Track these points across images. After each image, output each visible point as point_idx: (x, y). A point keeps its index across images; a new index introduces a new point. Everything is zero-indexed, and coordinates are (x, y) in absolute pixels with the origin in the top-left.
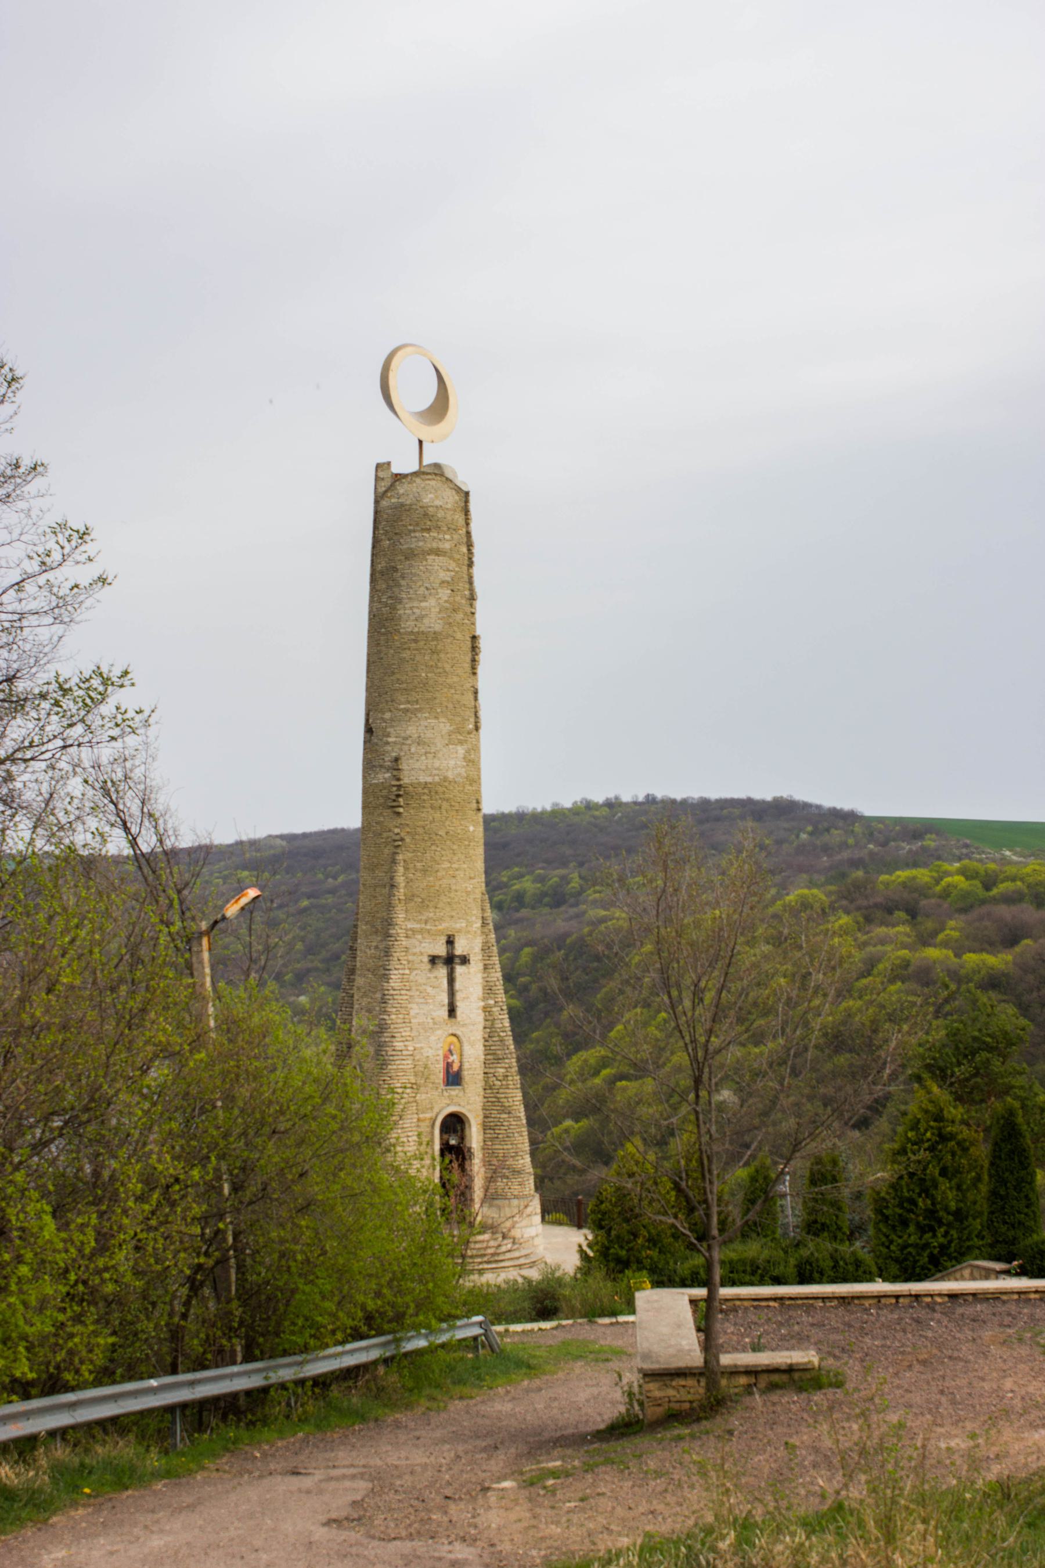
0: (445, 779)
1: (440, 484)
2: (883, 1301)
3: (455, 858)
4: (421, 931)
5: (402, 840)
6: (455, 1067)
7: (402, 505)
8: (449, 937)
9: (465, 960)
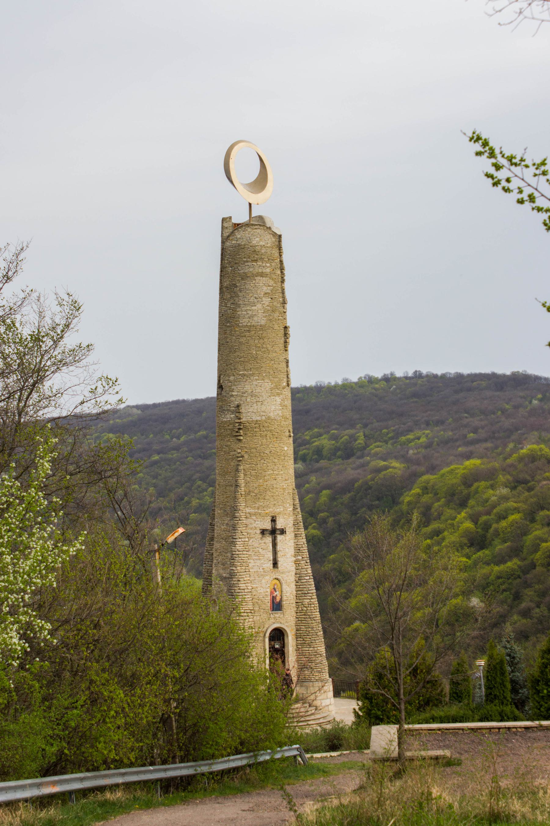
0: (269, 418)
1: (263, 231)
2: (492, 730)
3: (276, 468)
4: (255, 514)
5: (242, 457)
6: (278, 599)
7: (239, 245)
8: (273, 517)
9: (283, 532)
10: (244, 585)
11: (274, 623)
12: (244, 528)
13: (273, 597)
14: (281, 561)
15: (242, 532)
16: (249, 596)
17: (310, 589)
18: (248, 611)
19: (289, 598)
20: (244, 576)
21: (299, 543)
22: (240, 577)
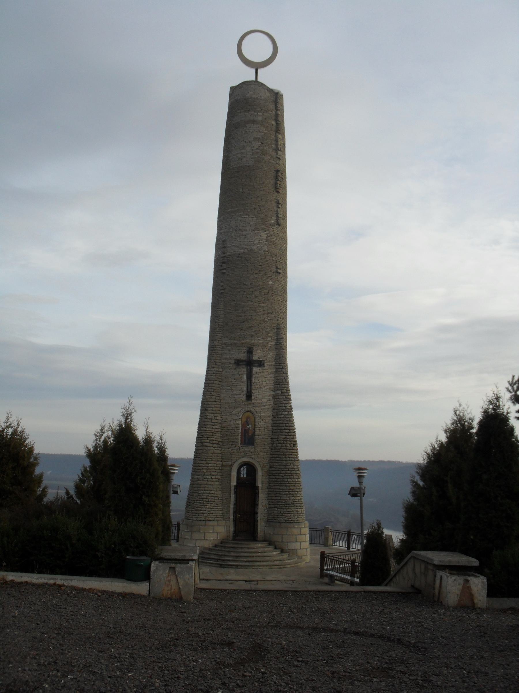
6: (250, 433)
9: (261, 364)
10: (212, 415)
11: (243, 457)
12: (218, 358)
13: (245, 430)
14: (255, 393)
15: (215, 362)
16: (217, 427)
17: (287, 425)
18: (214, 442)
19: (263, 433)
20: (213, 406)
21: (279, 378)
22: (208, 406)
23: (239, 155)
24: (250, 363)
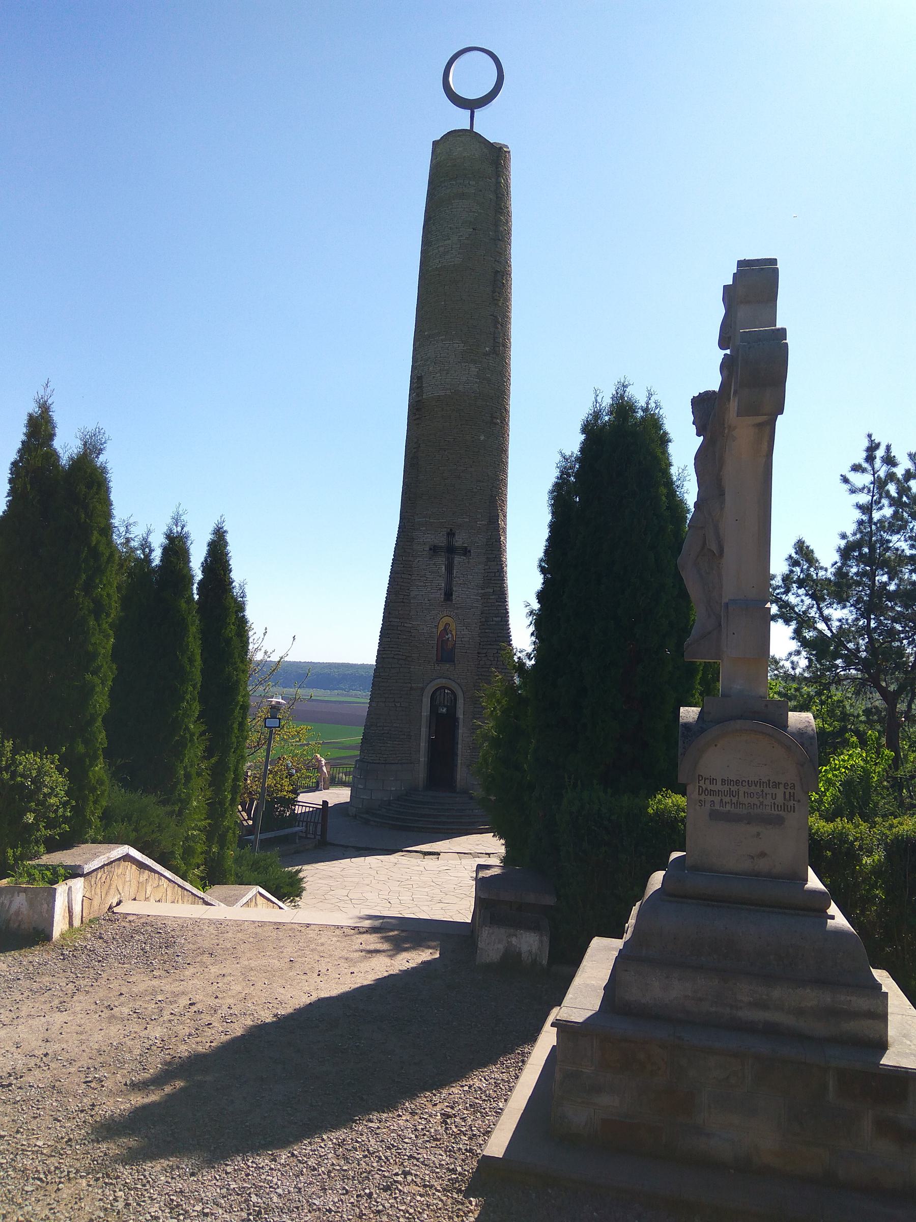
9: (466, 552)
23: (441, 249)
24: (451, 550)
